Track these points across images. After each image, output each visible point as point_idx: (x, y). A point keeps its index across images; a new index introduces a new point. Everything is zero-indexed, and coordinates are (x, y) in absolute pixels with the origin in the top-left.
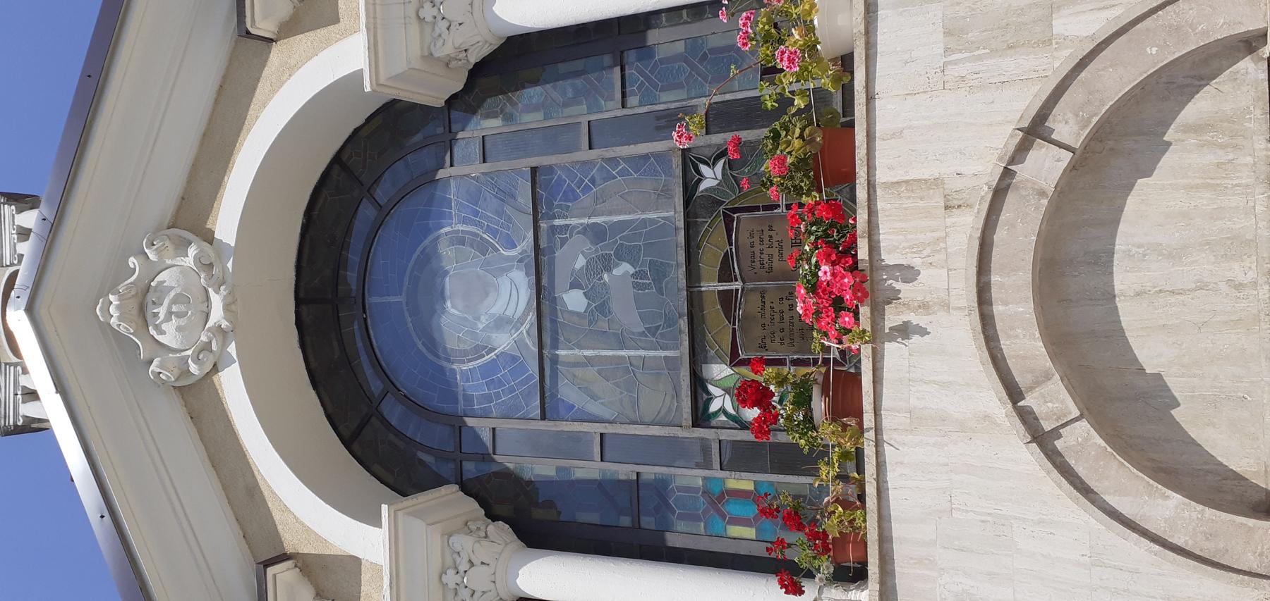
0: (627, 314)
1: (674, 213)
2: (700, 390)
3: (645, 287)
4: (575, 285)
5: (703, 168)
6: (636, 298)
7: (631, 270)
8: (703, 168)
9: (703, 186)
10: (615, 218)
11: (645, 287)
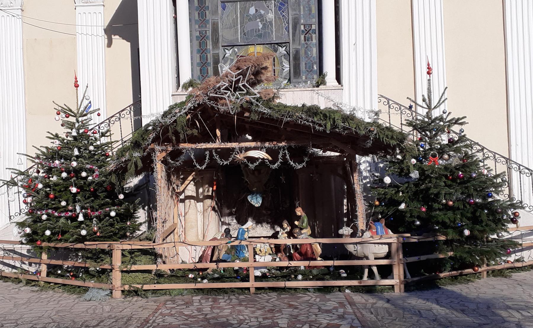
0: (249, 26)
1: (275, 40)
2: (231, 47)
3: (256, 32)
4: (256, 11)
5: (285, 48)
6: (253, 29)
7: (260, 28)
8: (285, 48)
9: (280, 48)
10: (274, 23)
11: (256, 32)
